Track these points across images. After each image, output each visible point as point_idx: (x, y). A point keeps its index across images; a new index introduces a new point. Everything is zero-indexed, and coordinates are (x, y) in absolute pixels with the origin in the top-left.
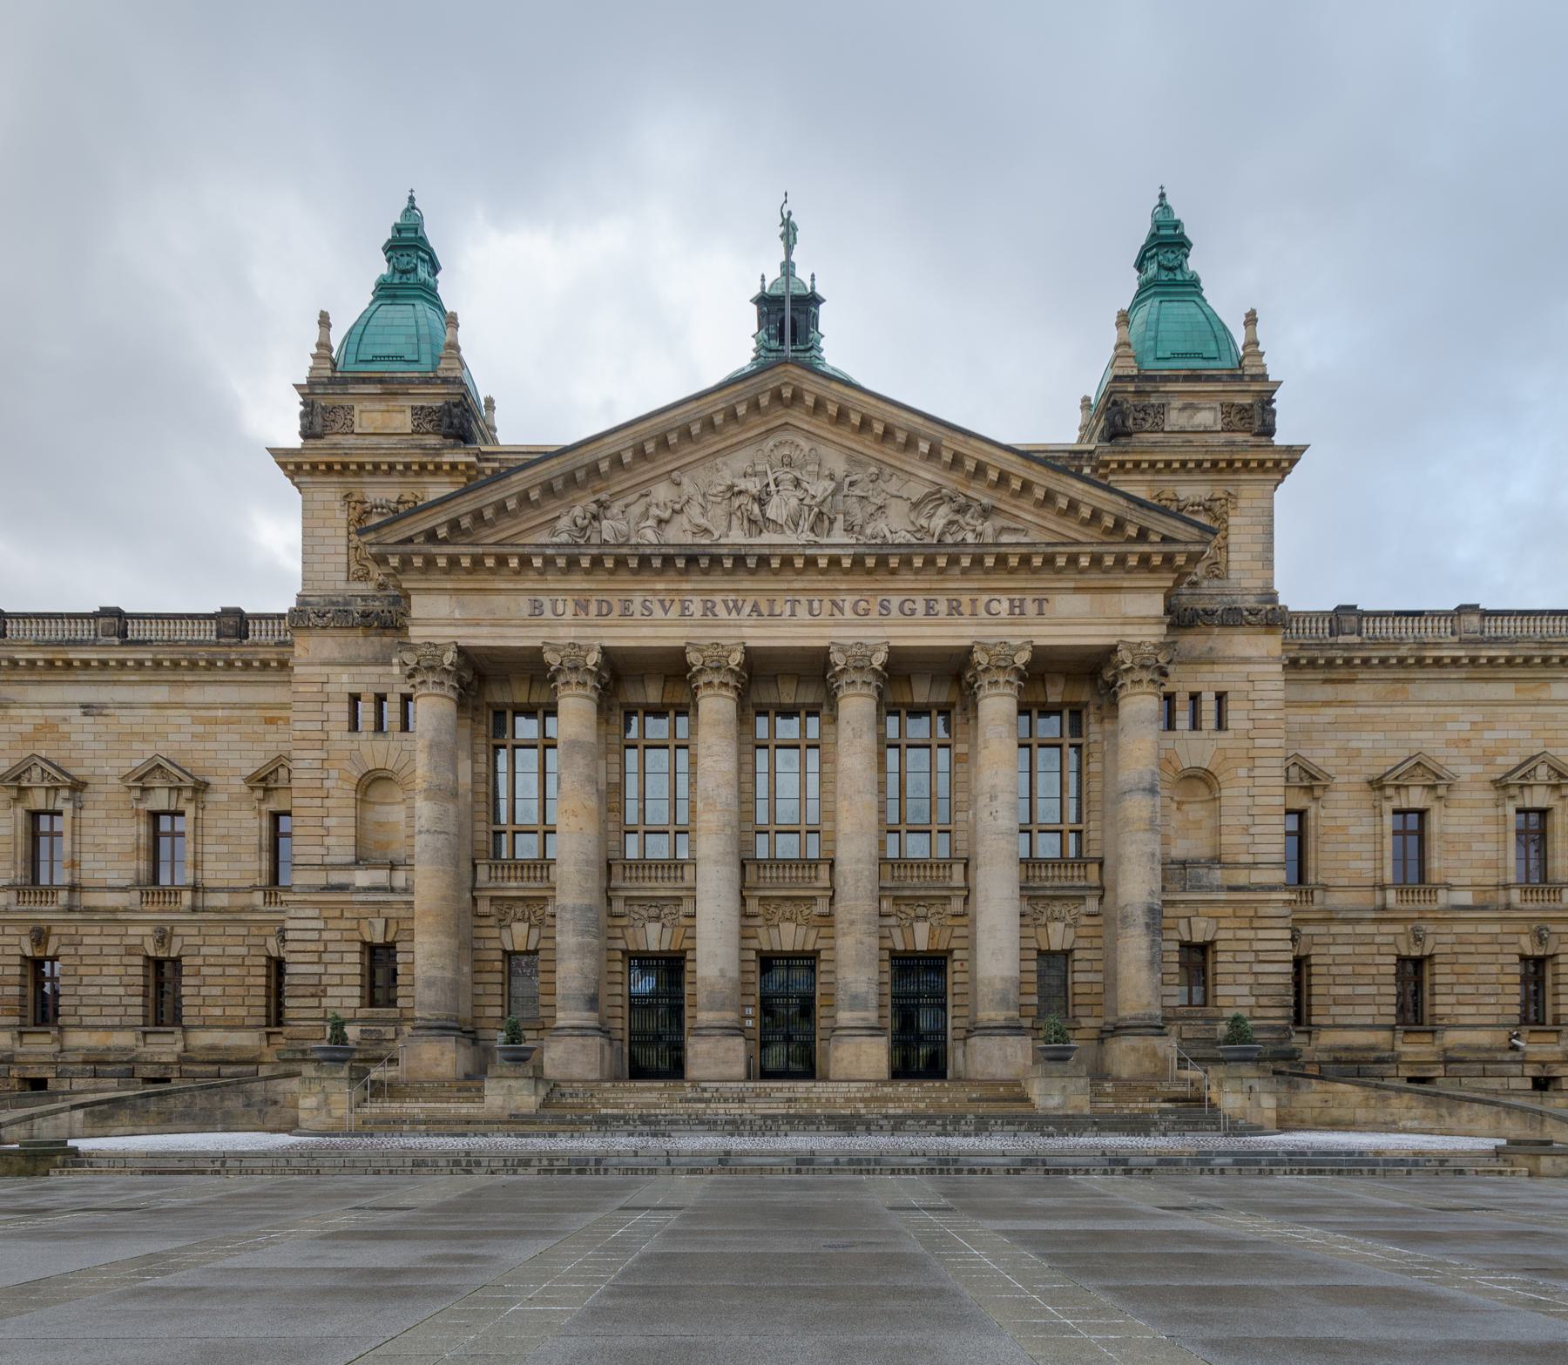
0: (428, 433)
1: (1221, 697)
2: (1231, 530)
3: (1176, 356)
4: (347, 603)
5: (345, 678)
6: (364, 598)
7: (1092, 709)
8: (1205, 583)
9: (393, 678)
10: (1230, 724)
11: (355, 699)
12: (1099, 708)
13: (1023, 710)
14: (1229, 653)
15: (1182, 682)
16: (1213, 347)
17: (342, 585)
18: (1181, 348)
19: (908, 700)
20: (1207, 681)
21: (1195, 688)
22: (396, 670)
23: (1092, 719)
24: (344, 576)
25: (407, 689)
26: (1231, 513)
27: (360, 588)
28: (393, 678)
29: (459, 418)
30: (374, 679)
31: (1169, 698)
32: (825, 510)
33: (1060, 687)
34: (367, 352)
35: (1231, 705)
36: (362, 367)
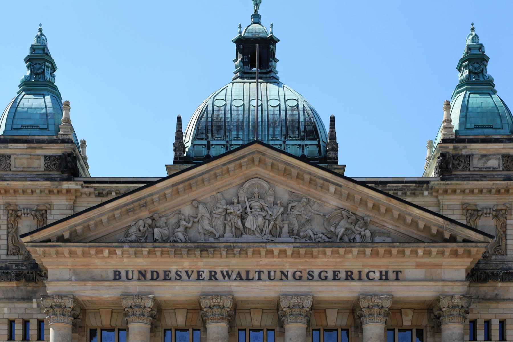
0: (53, 170)
1: (502, 323)
2: (508, 227)
3: (477, 127)
4: (7, 268)
5: (6, 310)
6: (17, 265)
7: (428, 329)
8: (493, 258)
9: (32, 309)
10: (508, 338)
11: (11, 323)
12: (433, 327)
13: (389, 329)
14: (505, 297)
15: (481, 313)
16: (498, 121)
17: (4, 257)
18: (480, 122)
19: (324, 323)
20: (494, 313)
21: (487, 317)
22: (35, 305)
23: (428, 334)
24: (5, 252)
25: (40, 317)
26: (508, 217)
27: (15, 258)
28: (32, 309)
29: (69, 164)
30: (23, 311)
31: (473, 323)
32: (277, 222)
33: (410, 317)
34: (18, 124)
35: (508, 327)
36: (15, 132)
